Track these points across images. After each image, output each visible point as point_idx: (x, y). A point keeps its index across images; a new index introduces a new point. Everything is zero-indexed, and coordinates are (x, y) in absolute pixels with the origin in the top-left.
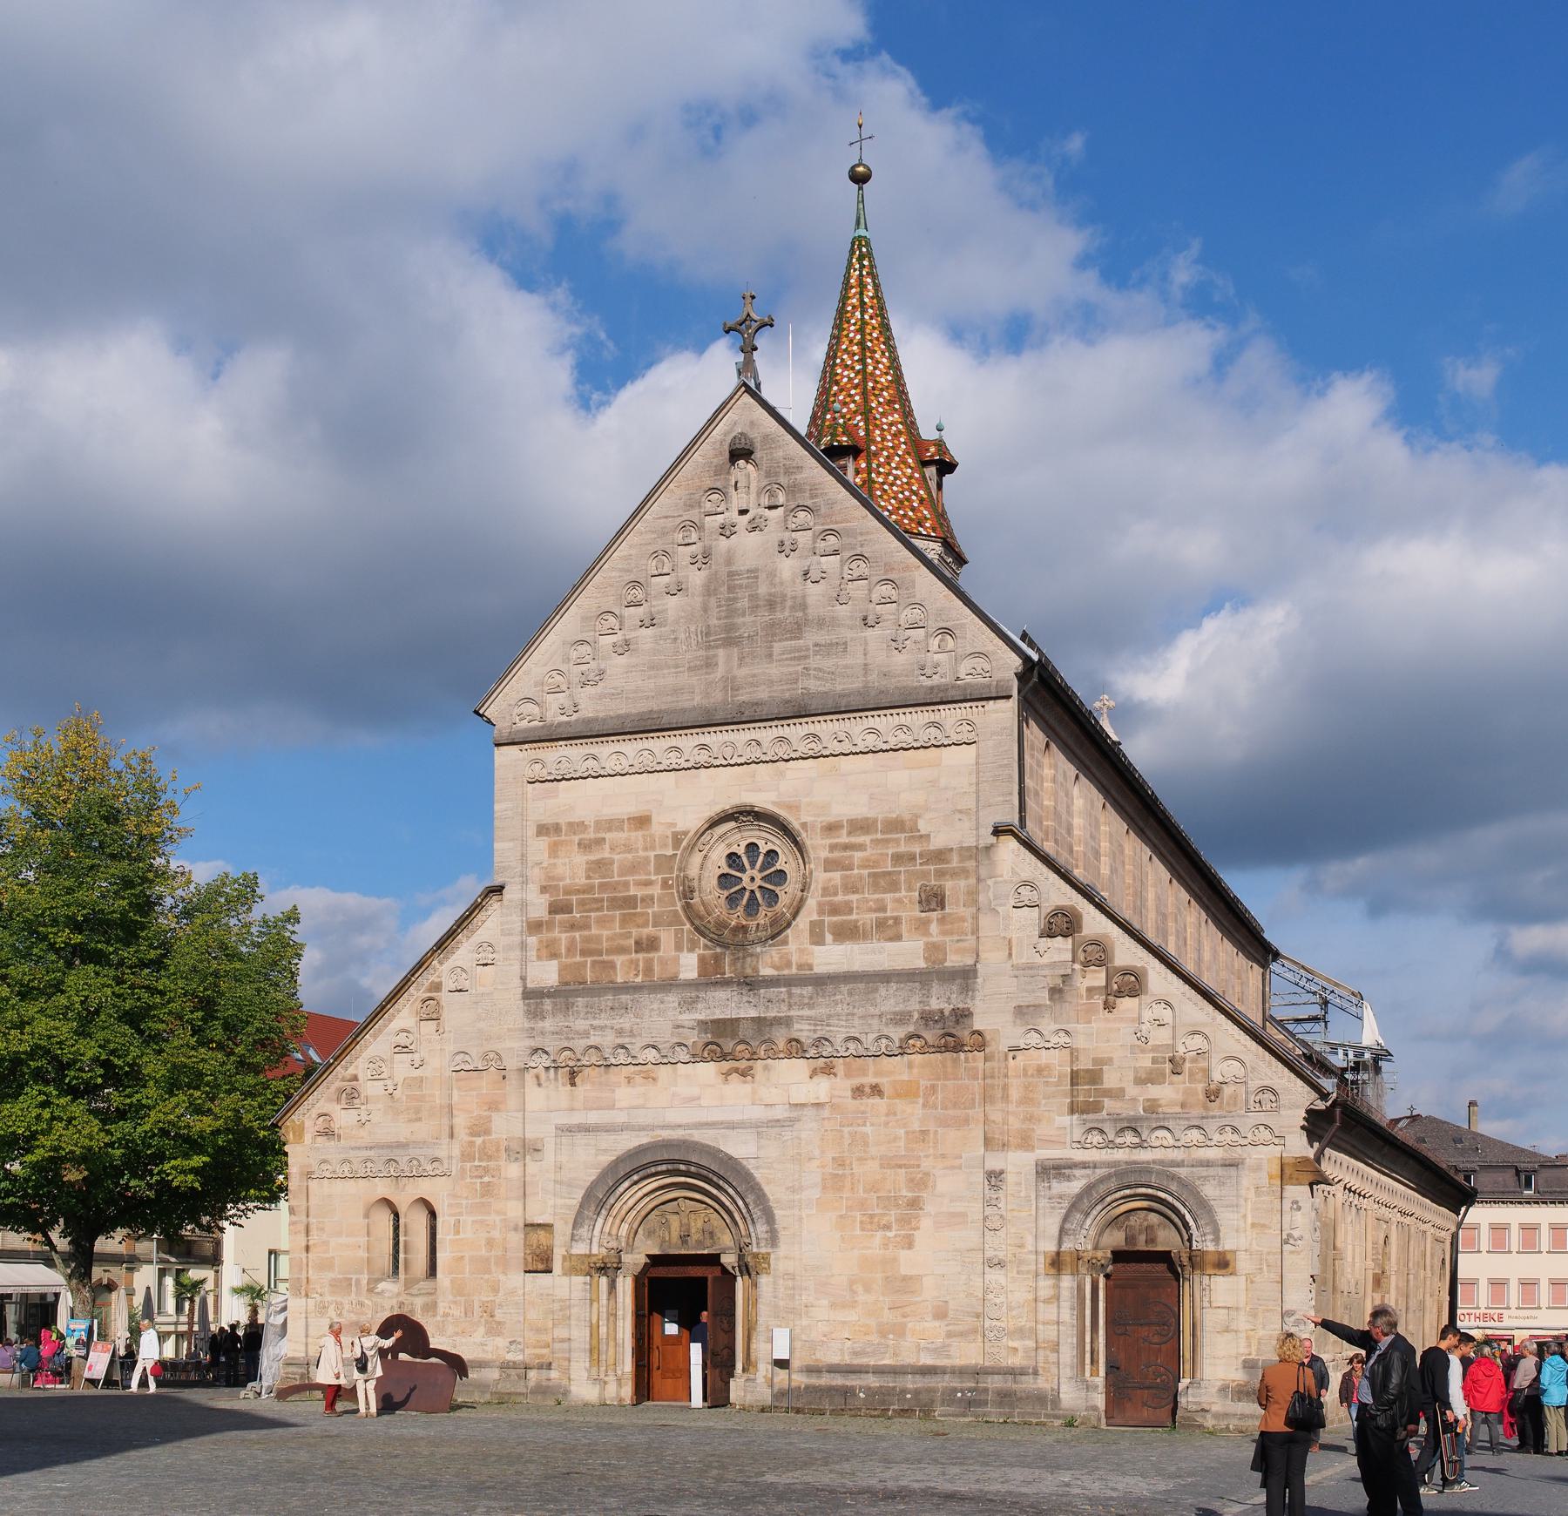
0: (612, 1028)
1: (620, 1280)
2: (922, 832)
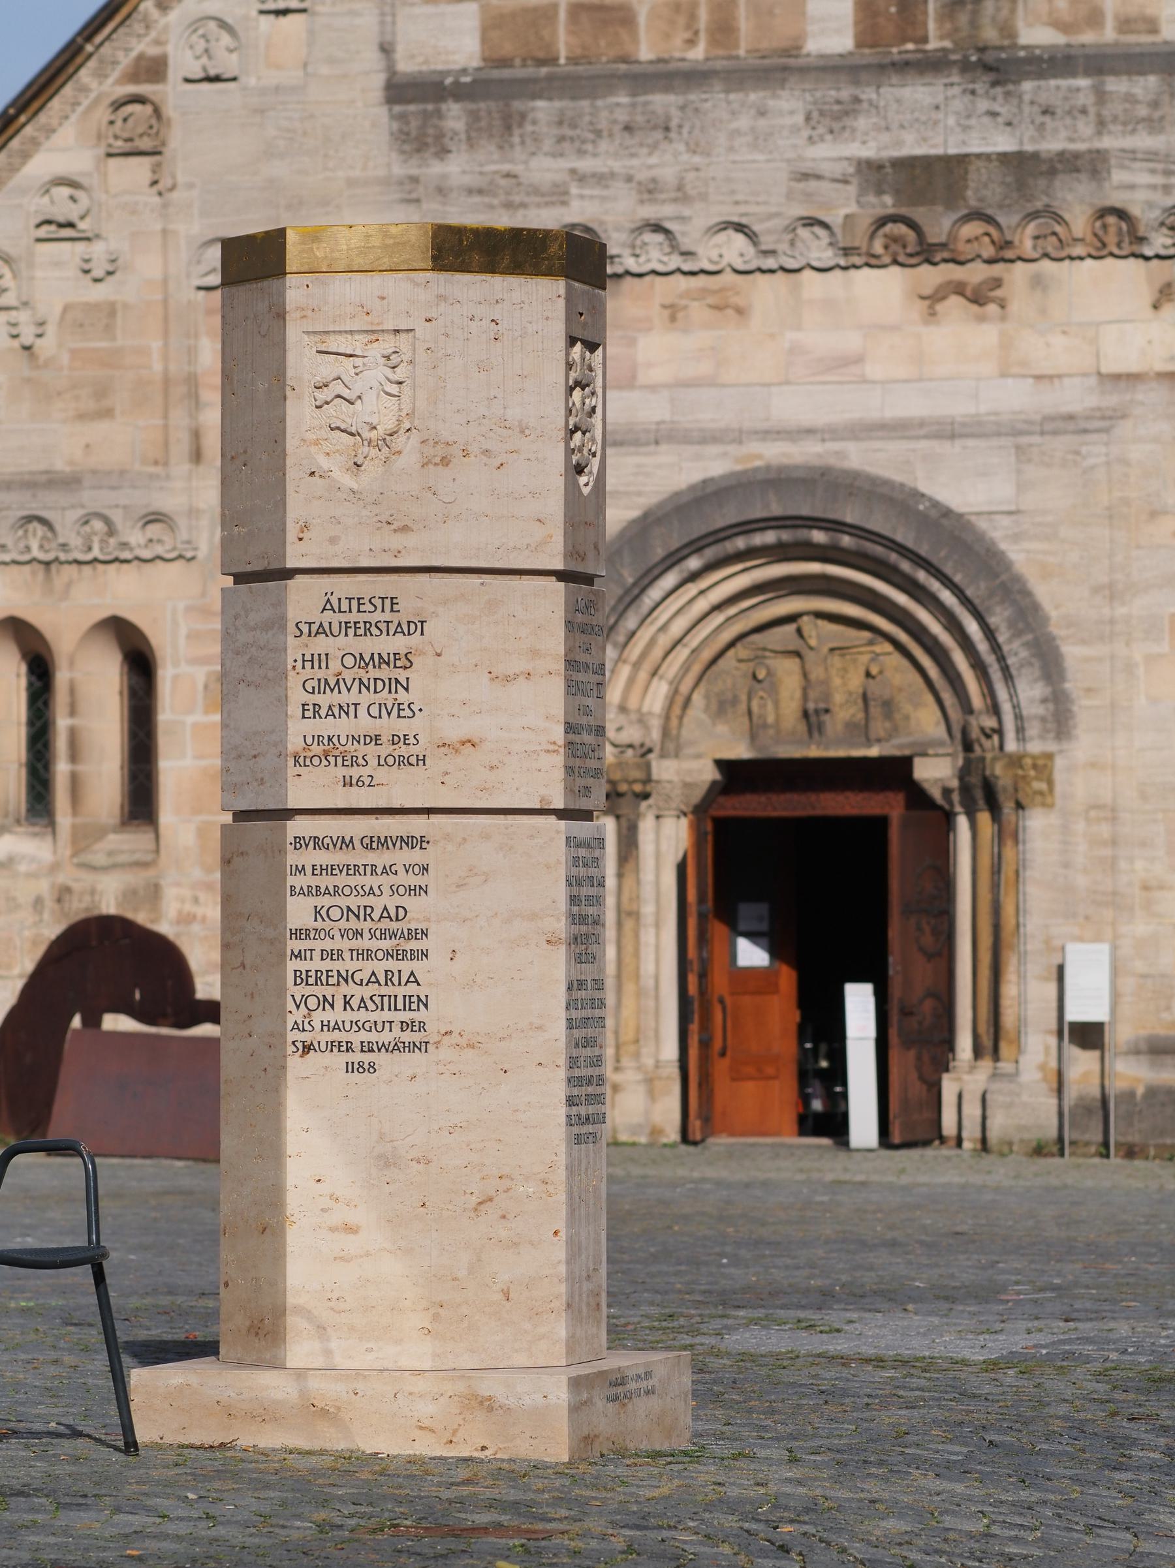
0: (629, 179)
1: (647, 826)
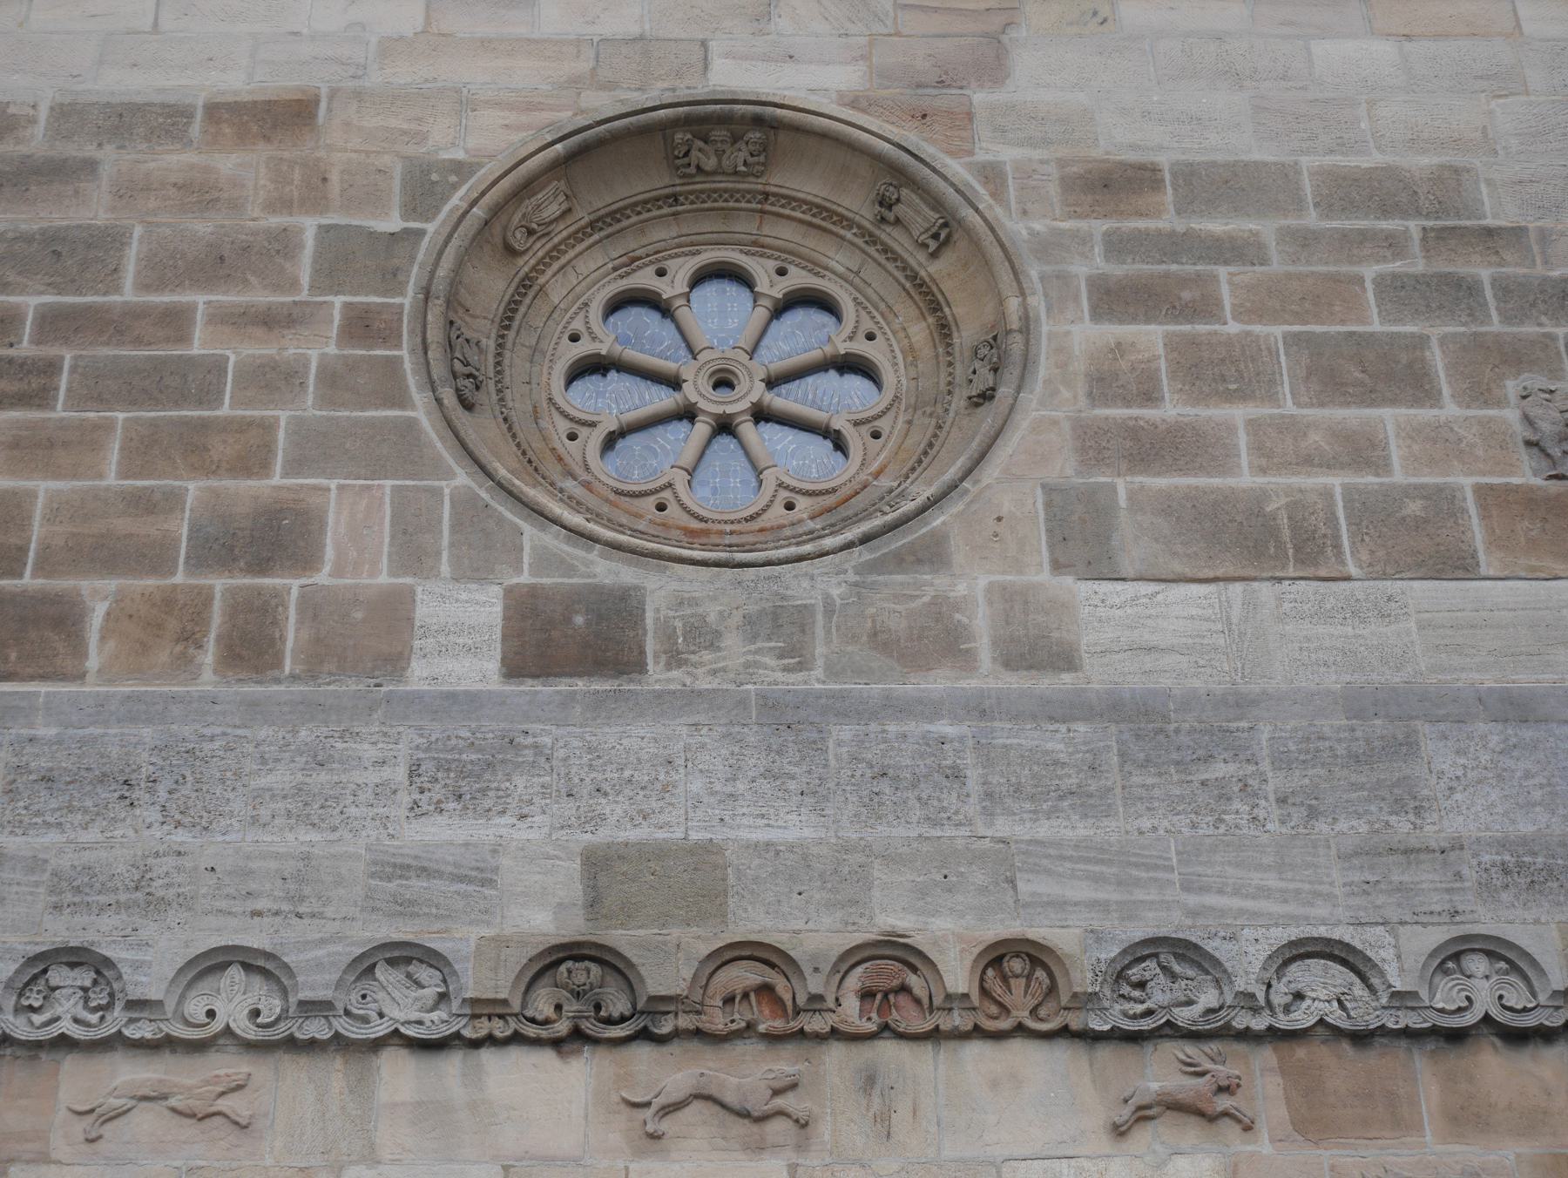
2: (1489, 222)
